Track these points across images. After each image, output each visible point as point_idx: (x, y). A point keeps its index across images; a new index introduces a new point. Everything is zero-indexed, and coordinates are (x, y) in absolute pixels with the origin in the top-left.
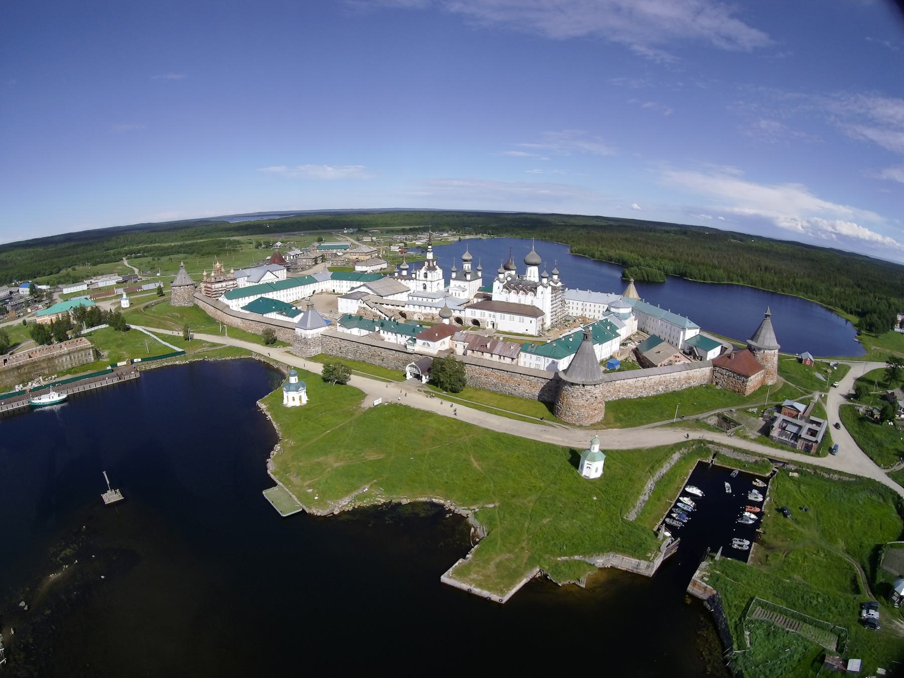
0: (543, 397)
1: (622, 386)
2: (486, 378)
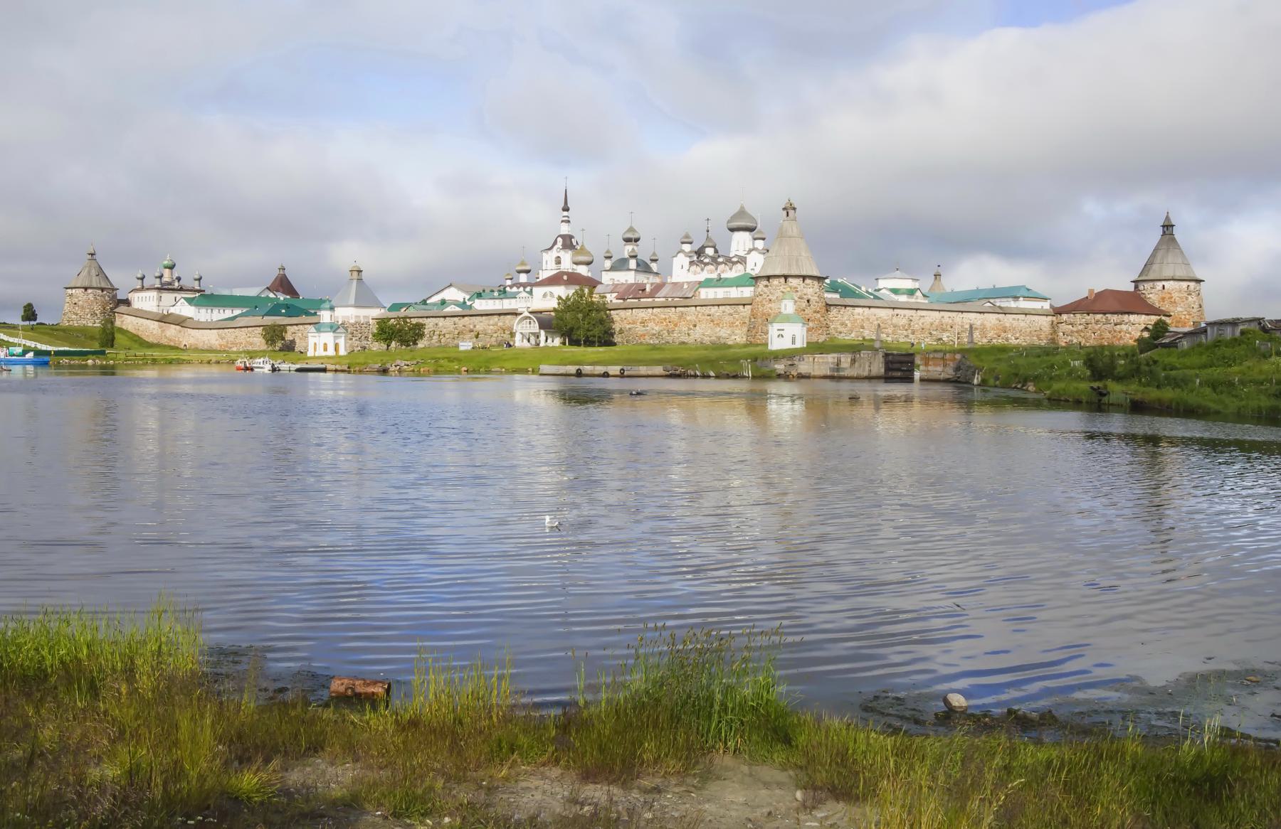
0: (733, 337)
1: (868, 319)
2: (644, 326)
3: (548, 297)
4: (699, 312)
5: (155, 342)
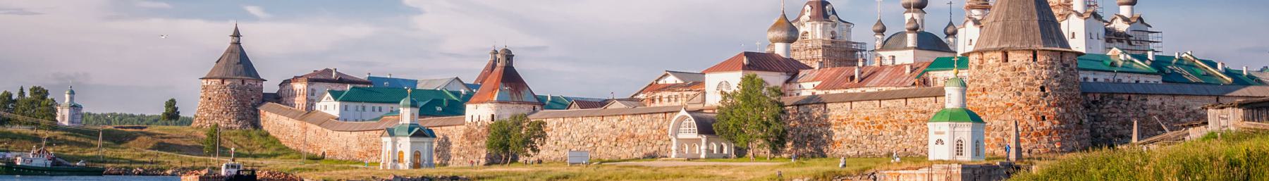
4: (910, 108)
5: (294, 148)
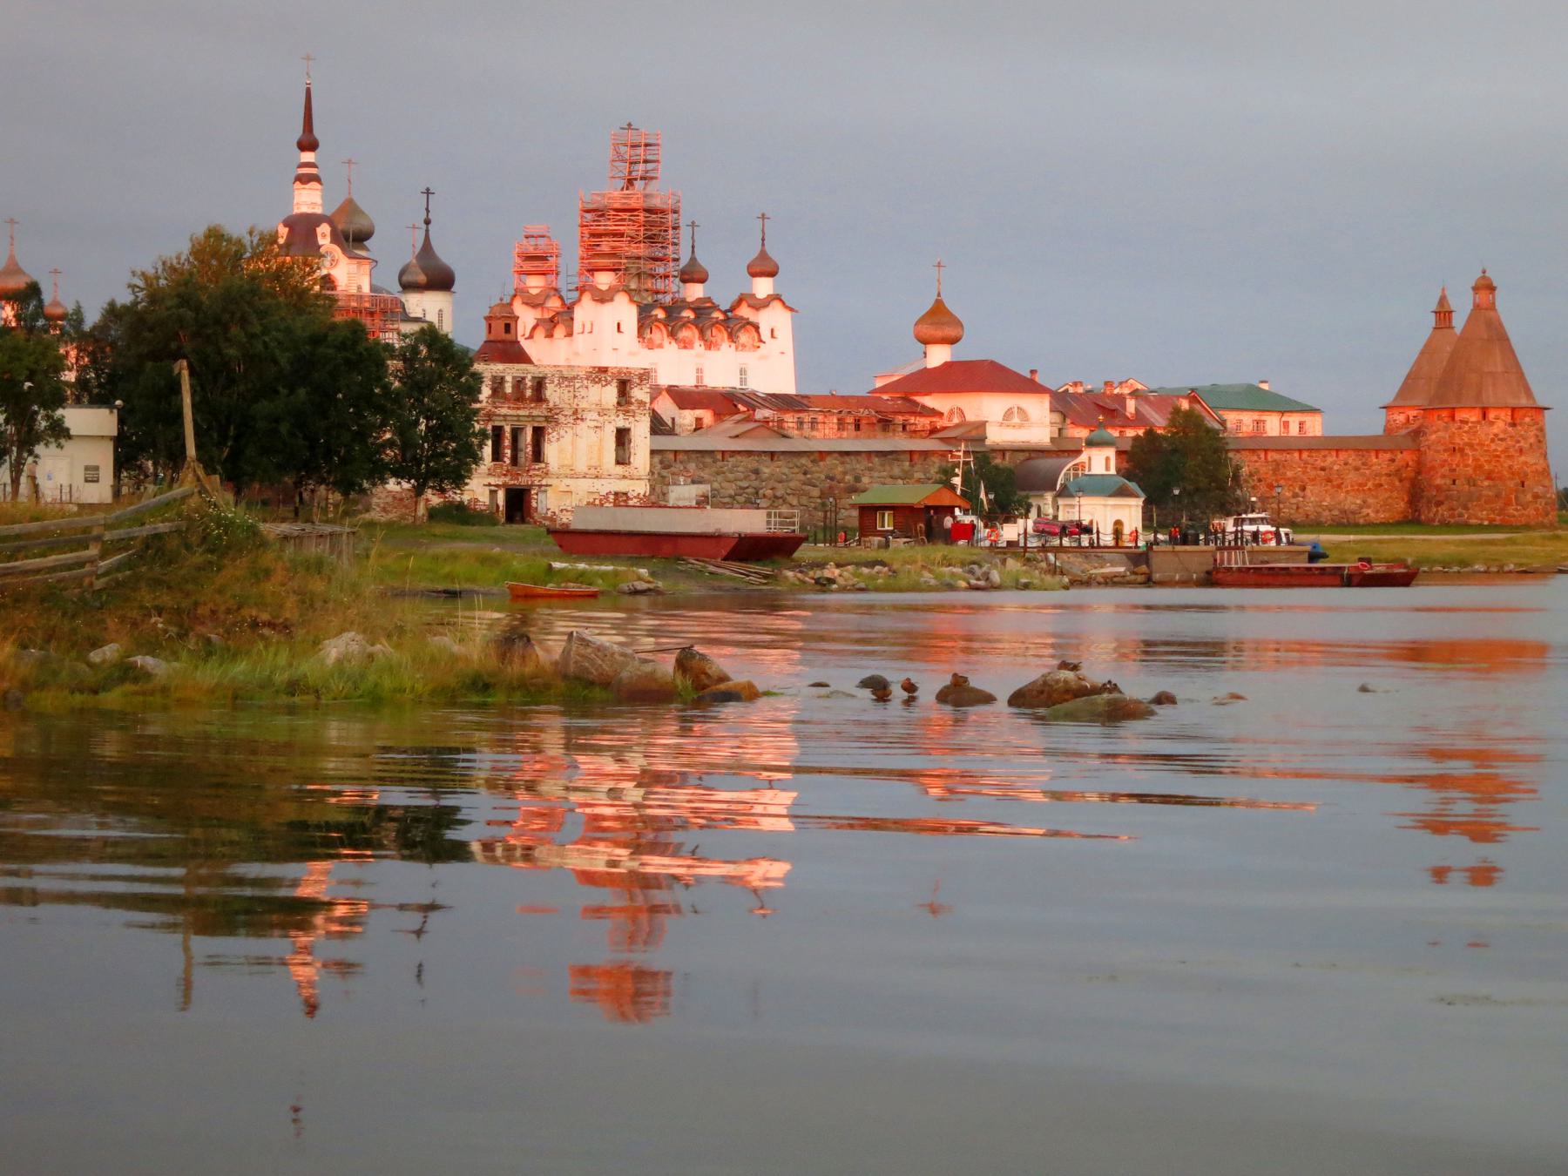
0: (1365, 511)
3: (1016, 420)
4: (1306, 463)
